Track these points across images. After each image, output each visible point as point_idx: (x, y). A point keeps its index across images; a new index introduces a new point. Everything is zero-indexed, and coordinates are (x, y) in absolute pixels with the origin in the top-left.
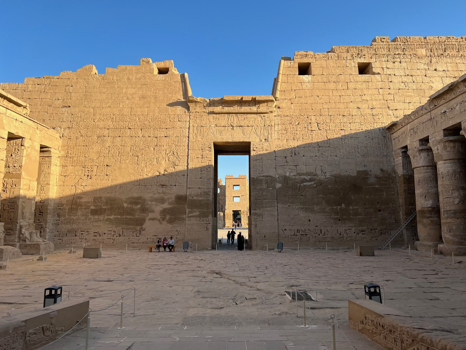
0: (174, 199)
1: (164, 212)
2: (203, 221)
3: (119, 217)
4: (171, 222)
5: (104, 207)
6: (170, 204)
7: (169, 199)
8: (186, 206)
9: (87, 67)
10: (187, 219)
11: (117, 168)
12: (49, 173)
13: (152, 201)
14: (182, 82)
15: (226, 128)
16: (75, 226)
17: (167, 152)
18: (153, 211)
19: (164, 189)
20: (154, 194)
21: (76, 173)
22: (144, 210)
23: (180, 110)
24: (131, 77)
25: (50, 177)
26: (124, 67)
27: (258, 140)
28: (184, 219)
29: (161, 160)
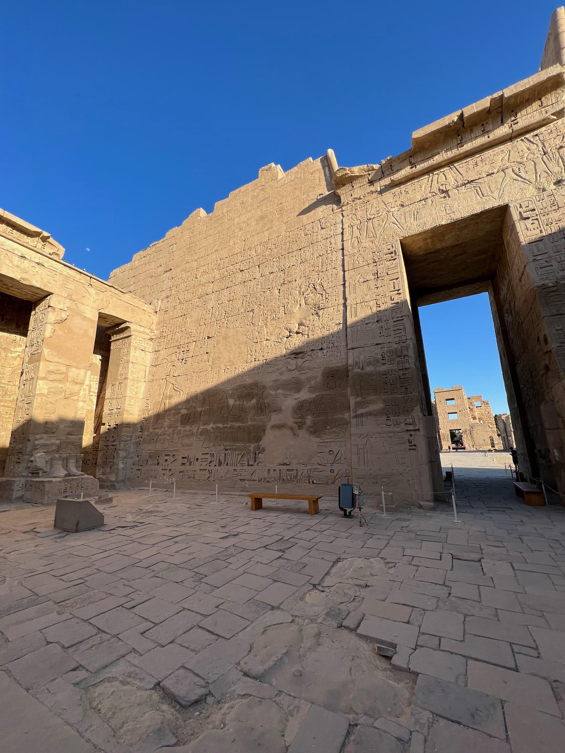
0: (319, 378)
1: (301, 409)
2: (397, 424)
3: (221, 425)
4: (315, 431)
5: (199, 409)
6: (312, 389)
7: (309, 379)
8: (349, 389)
9: (194, 213)
10: (353, 421)
11: (221, 338)
12: (128, 362)
13: (276, 389)
14: (324, 168)
15: (429, 201)
16: (159, 446)
17: (303, 290)
18: (278, 410)
19: (300, 361)
20: (281, 374)
21: (169, 358)
22: (263, 408)
23: (322, 211)
24: (245, 200)
25: (128, 368)
26: (237, 191)
27: (531, 191)
28: (347, 423)
29: (291, 307)
